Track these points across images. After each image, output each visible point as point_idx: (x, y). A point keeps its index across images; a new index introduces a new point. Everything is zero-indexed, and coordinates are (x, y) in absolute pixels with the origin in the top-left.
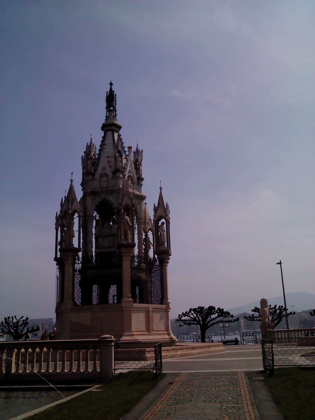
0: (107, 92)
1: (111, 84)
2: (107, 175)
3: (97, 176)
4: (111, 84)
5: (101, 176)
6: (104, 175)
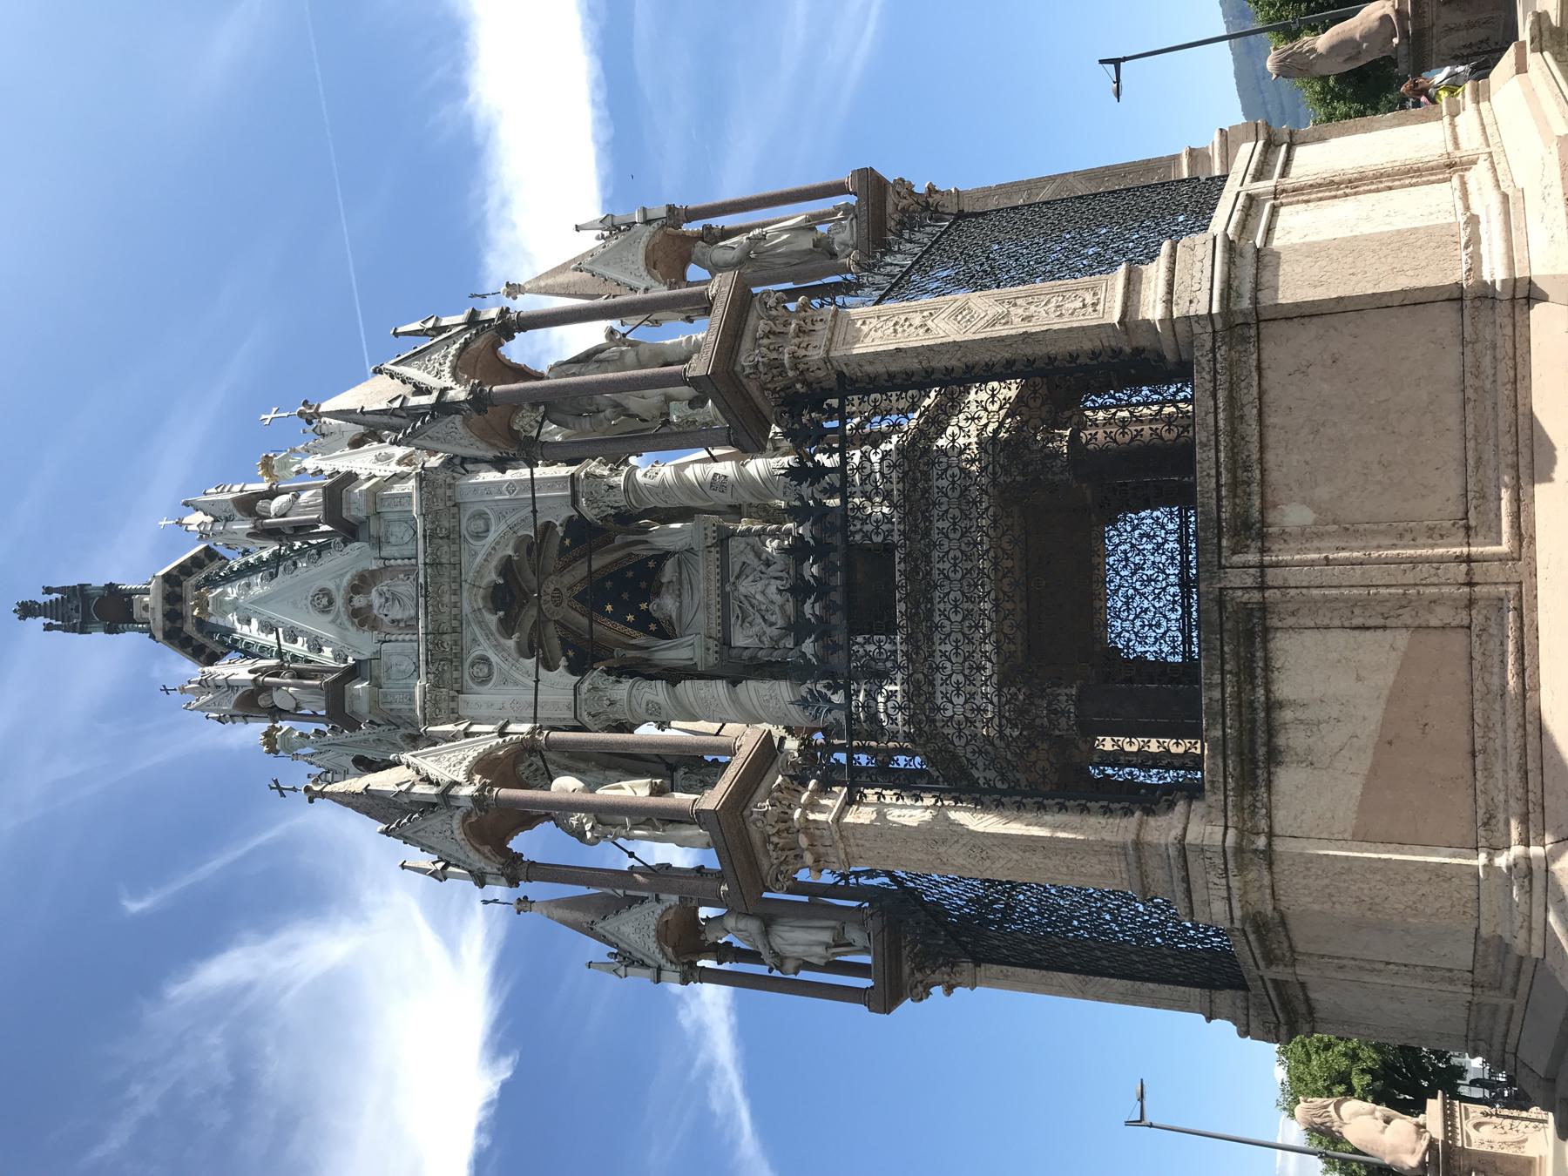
0: (48, 627)
1: (27, 610)
2: (362, 583)
3: (363, 644)
4: (27, 610)
5: (362, 618)
6: (359, 601)
